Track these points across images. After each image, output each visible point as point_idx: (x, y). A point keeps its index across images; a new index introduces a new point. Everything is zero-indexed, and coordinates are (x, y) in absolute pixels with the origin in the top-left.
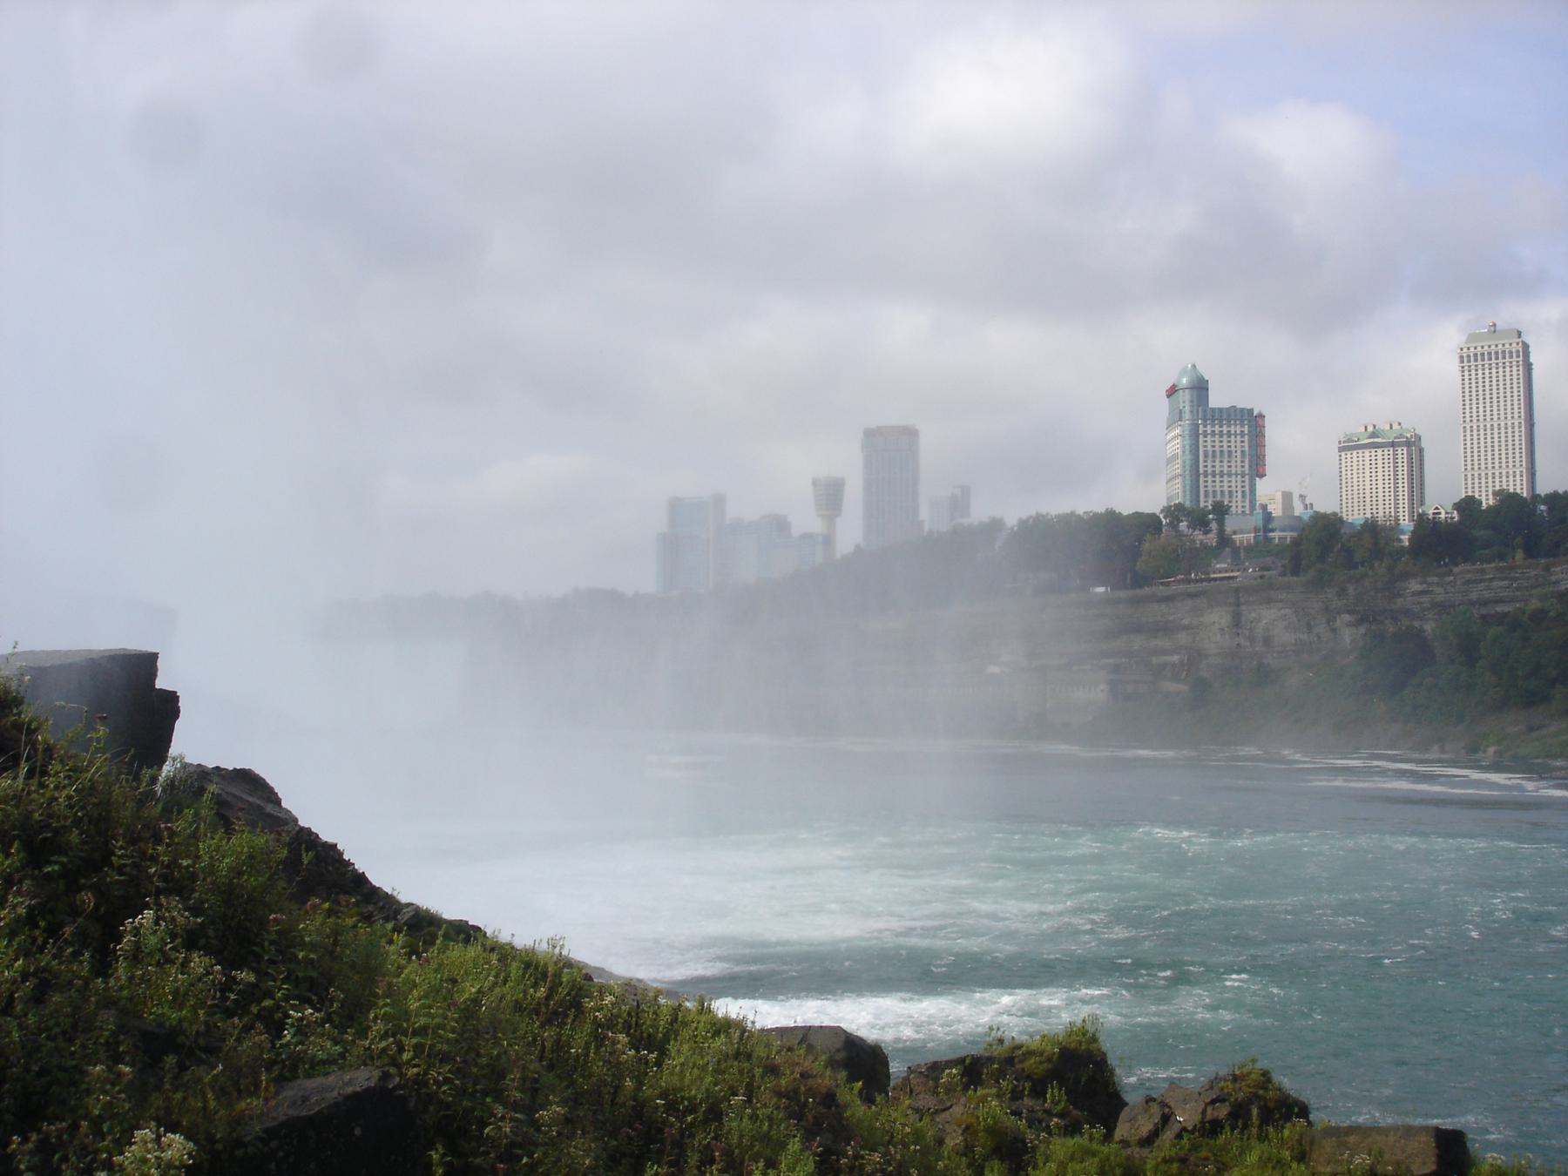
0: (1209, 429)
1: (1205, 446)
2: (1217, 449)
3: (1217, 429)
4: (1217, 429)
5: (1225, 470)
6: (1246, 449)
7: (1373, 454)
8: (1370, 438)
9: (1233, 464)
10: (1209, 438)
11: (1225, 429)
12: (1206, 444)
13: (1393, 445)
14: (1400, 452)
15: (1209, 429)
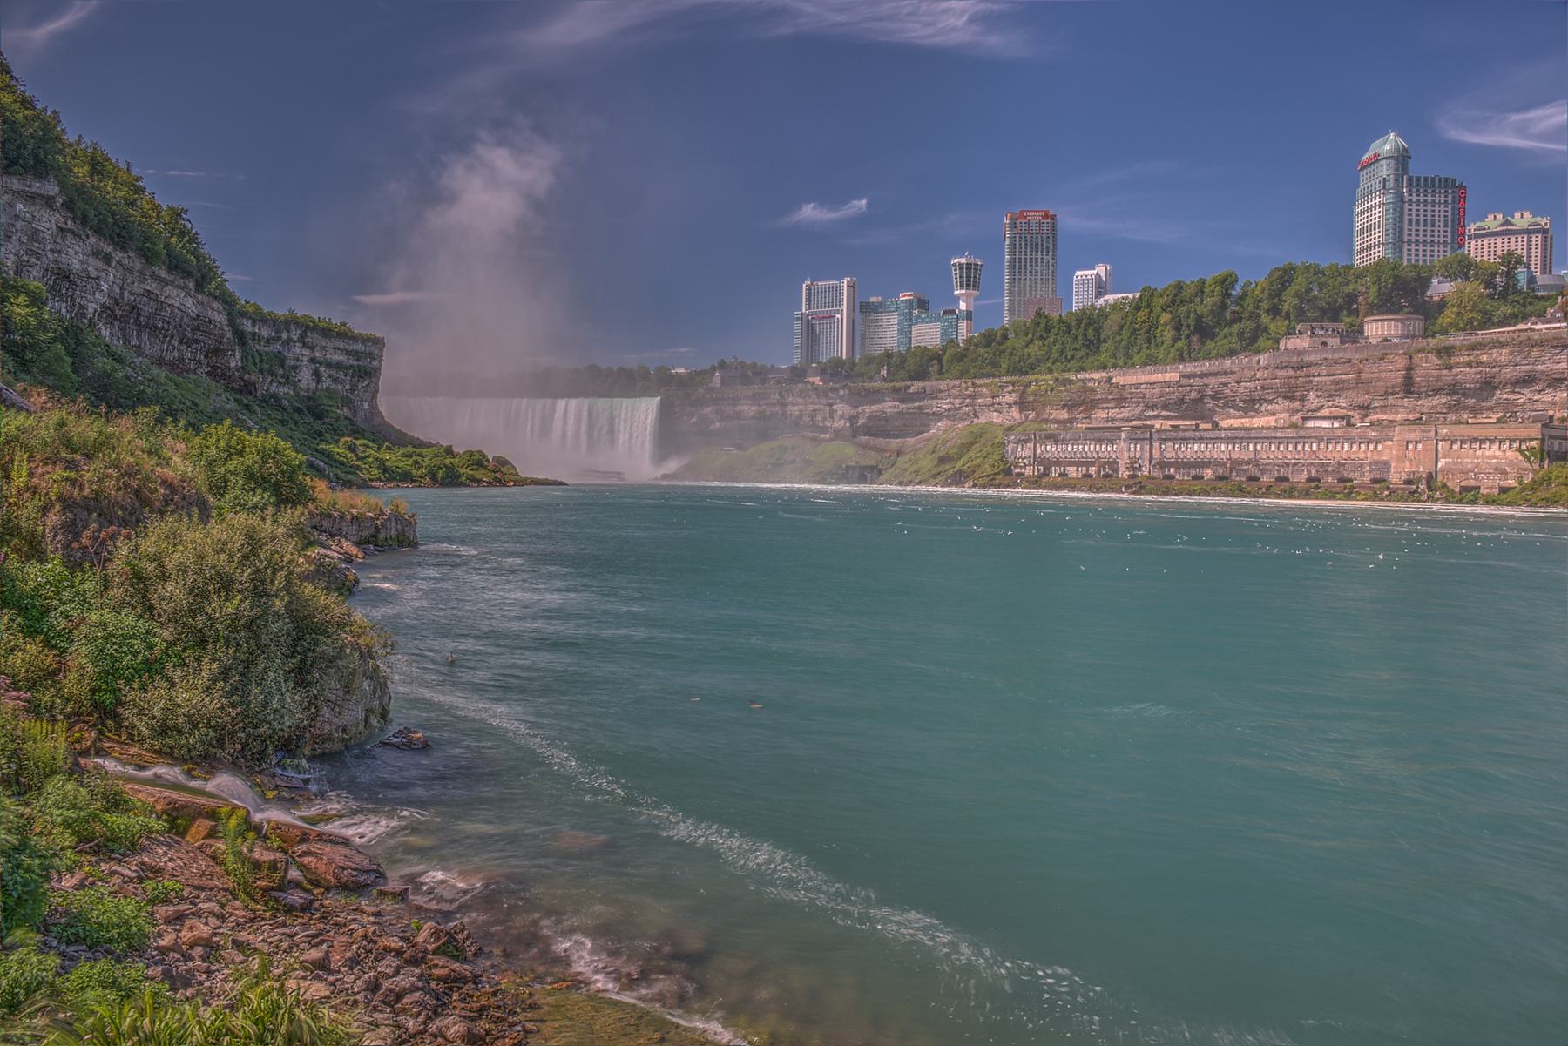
0: (1414, 198)
1: (1446, 211)
2: (1421, 218)
3: (1422, 198)
4: (1422, 198)
5: (1429, 239)
6: (1449, 219)
7: (1506, 240)
8: (1502, 225)
9: (1436, 234)
10: (1414, 207)
11: (1429, 198)
12: (1411, 212)
13: (1528, 232)
14: (1534, 239)
15: (1414, 198)
